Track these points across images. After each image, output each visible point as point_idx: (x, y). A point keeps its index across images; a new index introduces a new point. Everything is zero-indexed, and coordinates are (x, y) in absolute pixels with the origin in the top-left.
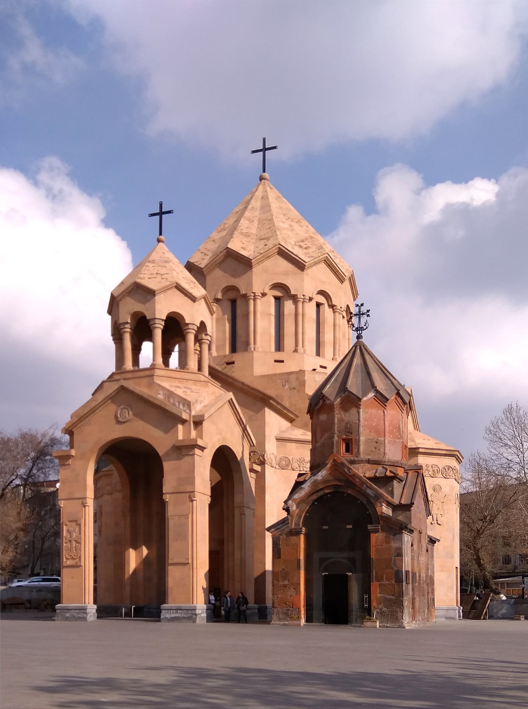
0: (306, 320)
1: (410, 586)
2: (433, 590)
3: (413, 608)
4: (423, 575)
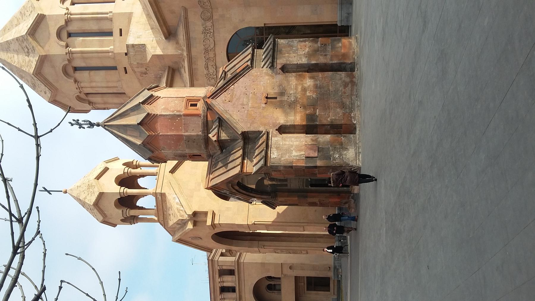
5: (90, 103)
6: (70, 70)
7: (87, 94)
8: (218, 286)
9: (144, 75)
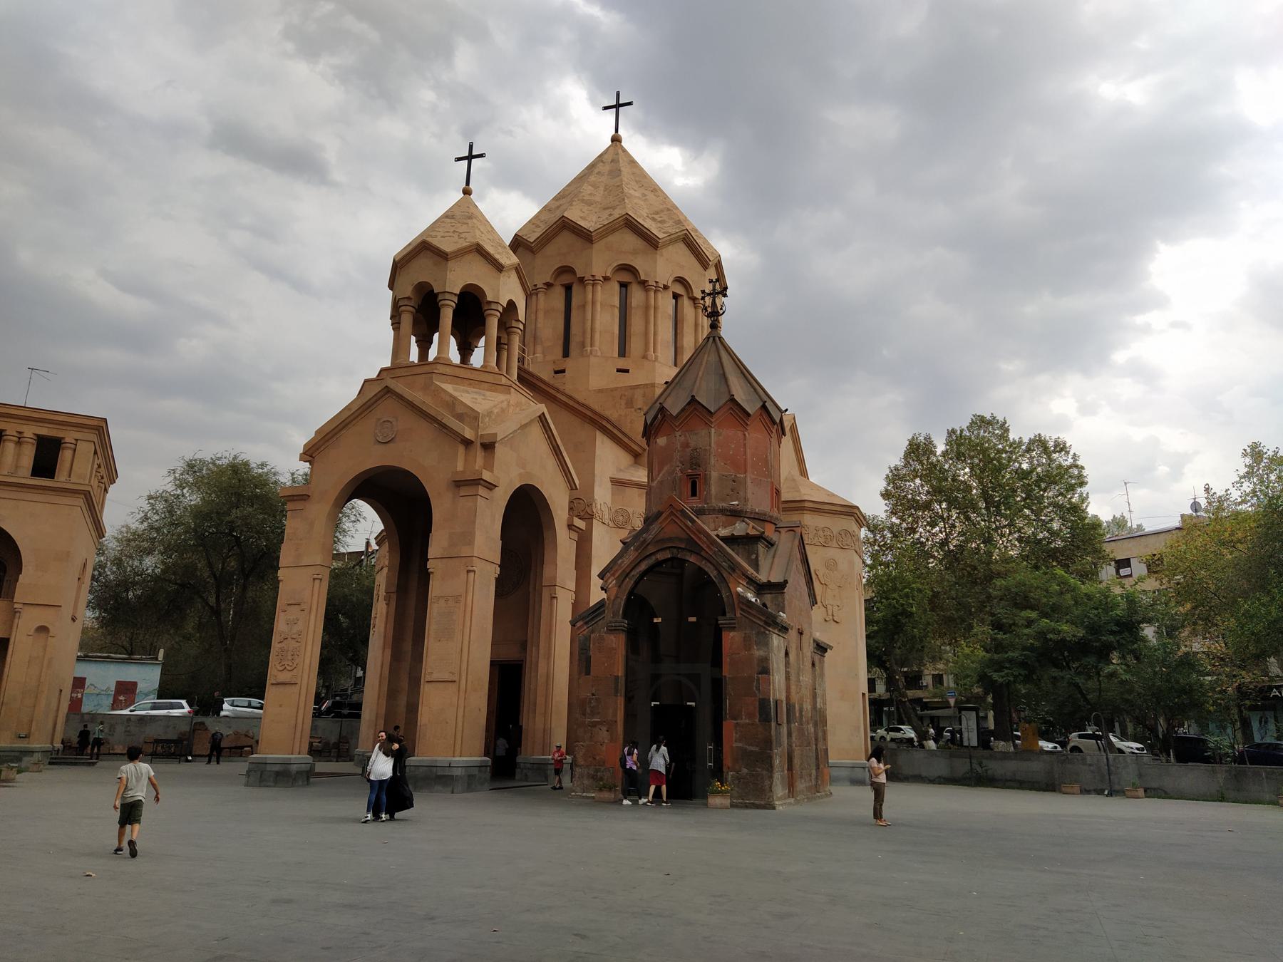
0: (659, 315)
1: (784, 730)
2: (825, 733)
3: (790, 768)
4: (807, 706)
5: (549, 285)
6: (625, 277)
7: (568, 288)
8: (11, 428)
9: (623, 402)
